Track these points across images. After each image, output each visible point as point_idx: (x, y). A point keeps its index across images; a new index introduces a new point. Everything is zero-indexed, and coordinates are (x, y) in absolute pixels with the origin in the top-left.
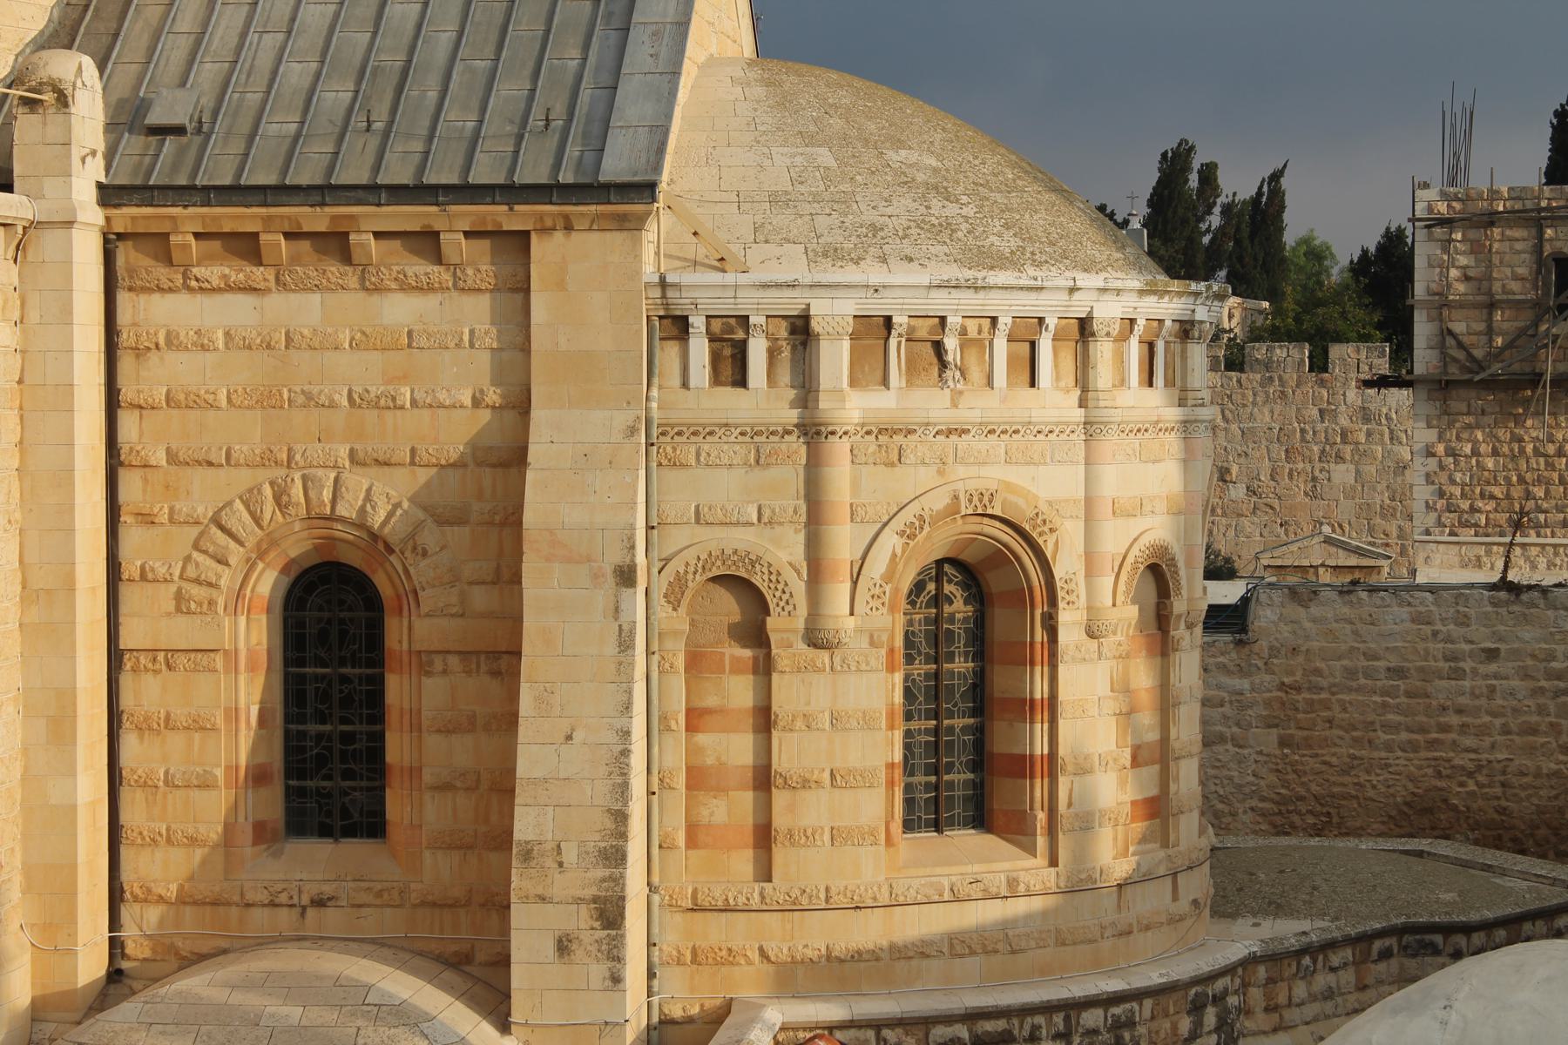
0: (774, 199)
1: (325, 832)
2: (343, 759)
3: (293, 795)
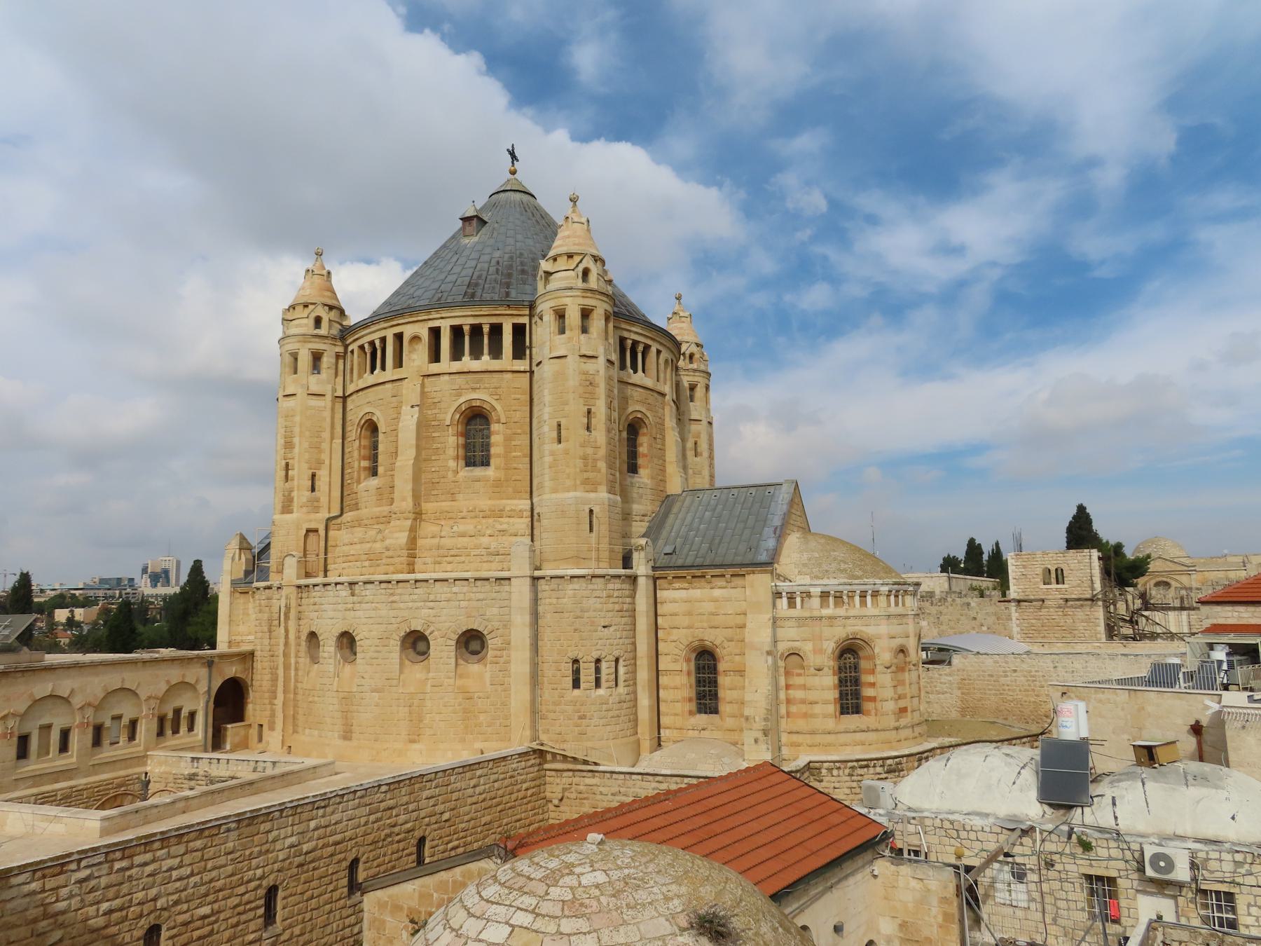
0: (805, 565)
1: (706, 713)
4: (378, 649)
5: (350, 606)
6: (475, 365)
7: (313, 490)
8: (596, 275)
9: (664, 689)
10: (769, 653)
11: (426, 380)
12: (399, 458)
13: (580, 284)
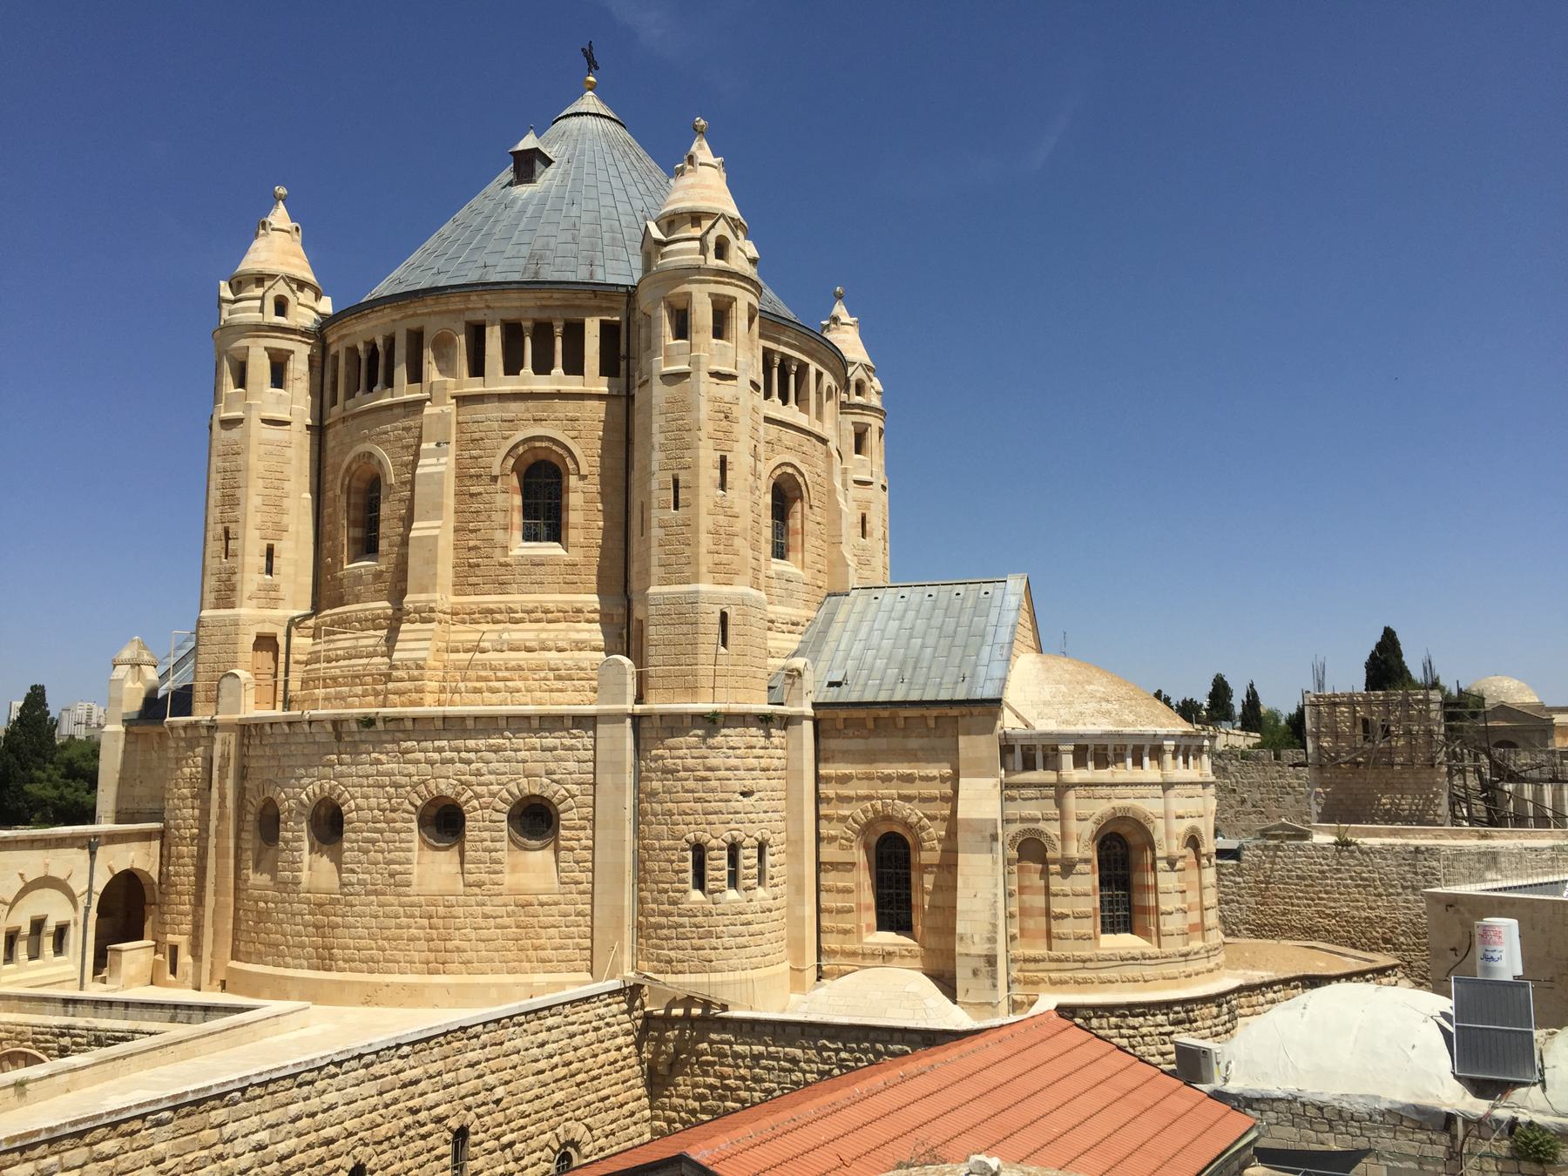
1: (891, 929)
2: (897, 902)
6: (542, 384)
7: (269, 571)
9: (827, 891)
12: (415, 525)
13: (713, 262)
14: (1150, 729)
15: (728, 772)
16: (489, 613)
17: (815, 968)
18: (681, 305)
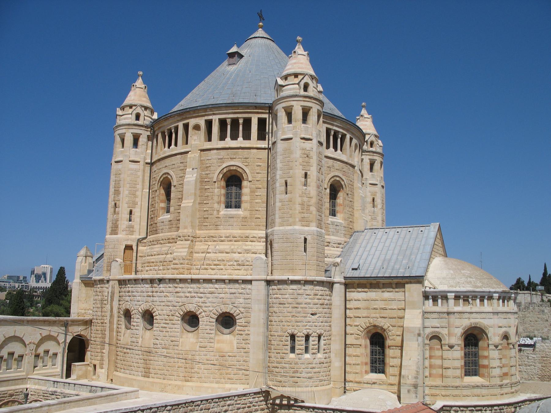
0: (444, 278)
1: (376, 372)
3: (372, 366)
4: (167, 322)
5: (150, 294)
8: (312, 87)
10: (419, 335)
11: (202, 152)
13: (302, 93)
14: (487, 289)
15: (306, 305)
16: (211, 237)
17: (343, 388)
18: (289, 111)
